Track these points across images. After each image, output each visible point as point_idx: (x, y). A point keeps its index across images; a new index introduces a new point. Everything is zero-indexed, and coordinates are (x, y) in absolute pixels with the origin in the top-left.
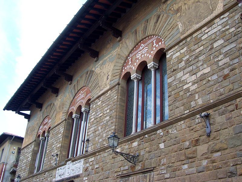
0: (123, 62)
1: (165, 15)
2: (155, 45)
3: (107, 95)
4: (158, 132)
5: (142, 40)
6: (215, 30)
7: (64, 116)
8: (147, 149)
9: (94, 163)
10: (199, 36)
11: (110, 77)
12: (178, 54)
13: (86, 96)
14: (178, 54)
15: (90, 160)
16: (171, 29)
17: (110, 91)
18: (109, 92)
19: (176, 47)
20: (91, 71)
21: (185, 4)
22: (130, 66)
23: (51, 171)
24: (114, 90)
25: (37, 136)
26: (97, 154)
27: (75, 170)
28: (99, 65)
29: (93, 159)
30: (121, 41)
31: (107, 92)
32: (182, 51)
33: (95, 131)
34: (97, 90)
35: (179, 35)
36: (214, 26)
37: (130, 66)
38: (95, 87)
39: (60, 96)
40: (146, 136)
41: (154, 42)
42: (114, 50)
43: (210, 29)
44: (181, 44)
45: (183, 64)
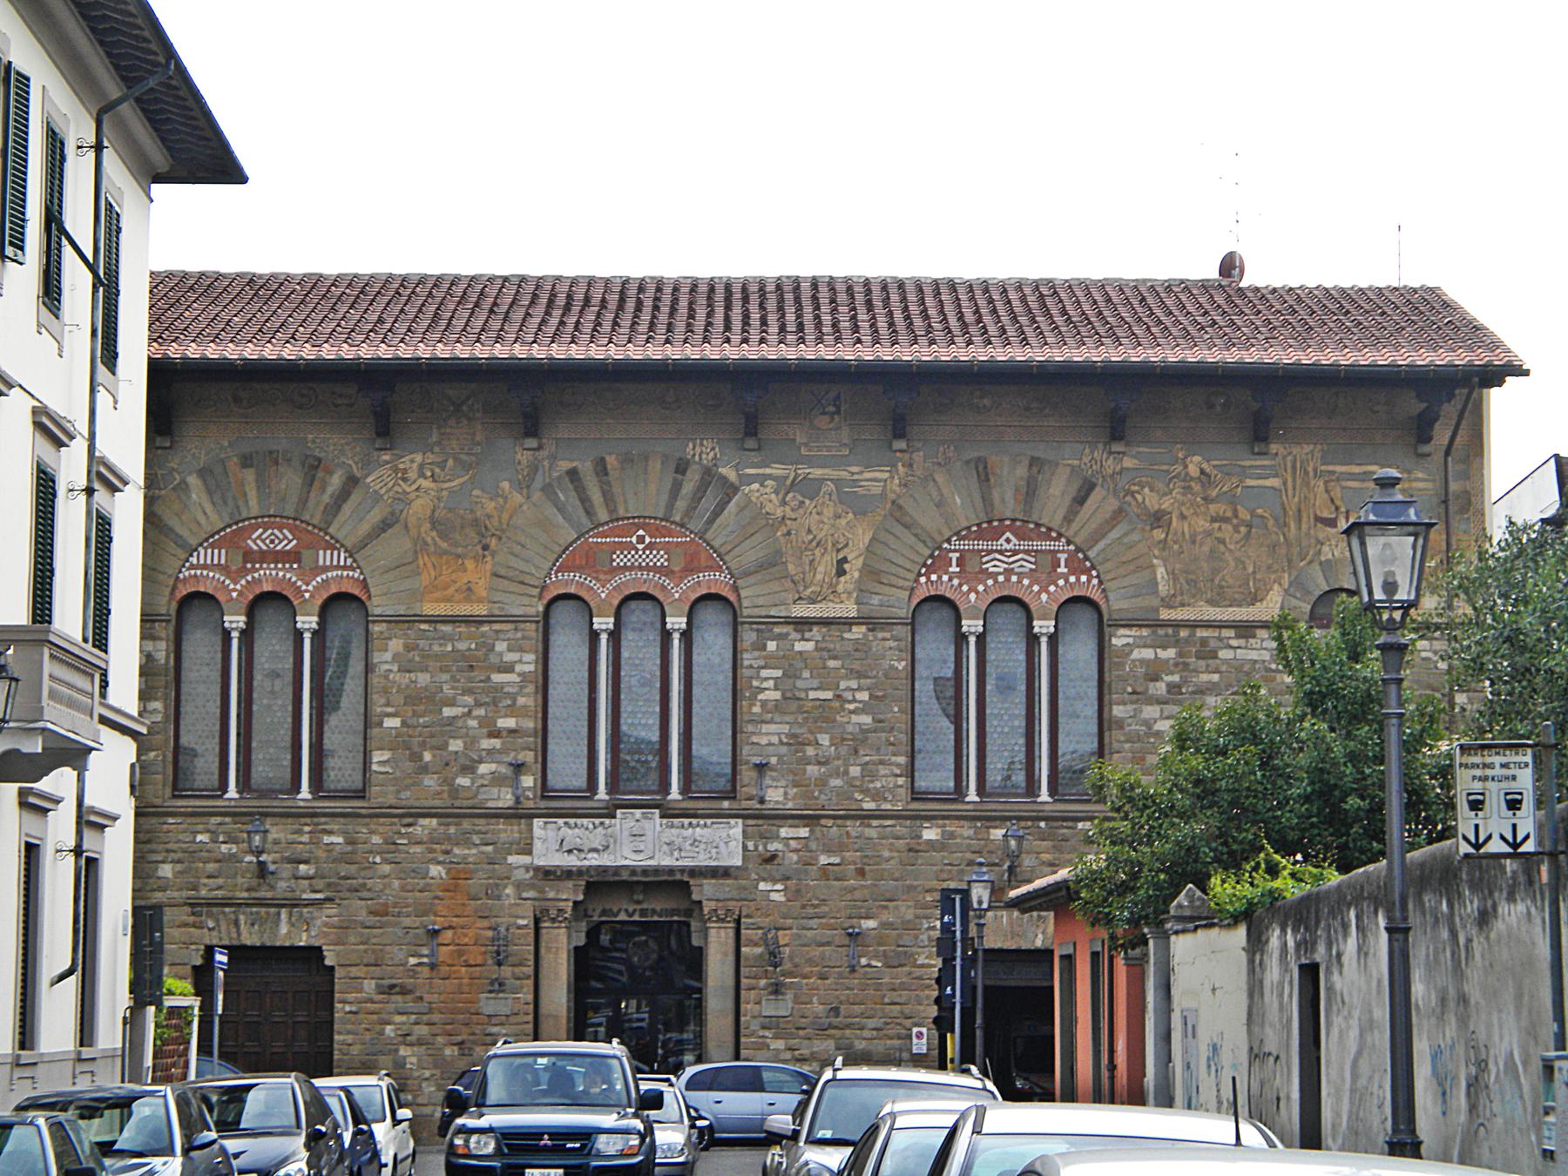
0: (927, 552)
1: (1113, 504)
2: (1062, 570)
3: (846, 635)
4: (1080, 825)
5: (1013, 520)
6: (1253, 655)
7: (526, 600)
8: (1046, 857)
9: (813, 846)
10: (1213, 644)
11: (853, 570)
12: (1148, 654)
13: (689, 570)
14: (1148, 654)
15: (784, 832)
16: (1132, 567)
17: (863, 629)
18: (854, 629)
19: (1145, 632)
20: (709, 474)
21: (1183, 517)
22: (956, 582)
23: (482, 821)
24: (888, 635)
26: (823, 822)
27: (687, 846)
28: (770, 477)
29: (804, 832)
30: (907, 456)
31: (848, 623)
32: (1162, 654)
33: (796, 742)
34: (775, 586)
35: (1156, 602)
36: (1251, 641)
37: (956, 582)
38: (762, 567)
39: (419, 458)
40: (1042, 824)
41: (1063, 557)
42: (868, 466)
43: (1242, 642)
44: (1161, 632)
45: (1160, 688)
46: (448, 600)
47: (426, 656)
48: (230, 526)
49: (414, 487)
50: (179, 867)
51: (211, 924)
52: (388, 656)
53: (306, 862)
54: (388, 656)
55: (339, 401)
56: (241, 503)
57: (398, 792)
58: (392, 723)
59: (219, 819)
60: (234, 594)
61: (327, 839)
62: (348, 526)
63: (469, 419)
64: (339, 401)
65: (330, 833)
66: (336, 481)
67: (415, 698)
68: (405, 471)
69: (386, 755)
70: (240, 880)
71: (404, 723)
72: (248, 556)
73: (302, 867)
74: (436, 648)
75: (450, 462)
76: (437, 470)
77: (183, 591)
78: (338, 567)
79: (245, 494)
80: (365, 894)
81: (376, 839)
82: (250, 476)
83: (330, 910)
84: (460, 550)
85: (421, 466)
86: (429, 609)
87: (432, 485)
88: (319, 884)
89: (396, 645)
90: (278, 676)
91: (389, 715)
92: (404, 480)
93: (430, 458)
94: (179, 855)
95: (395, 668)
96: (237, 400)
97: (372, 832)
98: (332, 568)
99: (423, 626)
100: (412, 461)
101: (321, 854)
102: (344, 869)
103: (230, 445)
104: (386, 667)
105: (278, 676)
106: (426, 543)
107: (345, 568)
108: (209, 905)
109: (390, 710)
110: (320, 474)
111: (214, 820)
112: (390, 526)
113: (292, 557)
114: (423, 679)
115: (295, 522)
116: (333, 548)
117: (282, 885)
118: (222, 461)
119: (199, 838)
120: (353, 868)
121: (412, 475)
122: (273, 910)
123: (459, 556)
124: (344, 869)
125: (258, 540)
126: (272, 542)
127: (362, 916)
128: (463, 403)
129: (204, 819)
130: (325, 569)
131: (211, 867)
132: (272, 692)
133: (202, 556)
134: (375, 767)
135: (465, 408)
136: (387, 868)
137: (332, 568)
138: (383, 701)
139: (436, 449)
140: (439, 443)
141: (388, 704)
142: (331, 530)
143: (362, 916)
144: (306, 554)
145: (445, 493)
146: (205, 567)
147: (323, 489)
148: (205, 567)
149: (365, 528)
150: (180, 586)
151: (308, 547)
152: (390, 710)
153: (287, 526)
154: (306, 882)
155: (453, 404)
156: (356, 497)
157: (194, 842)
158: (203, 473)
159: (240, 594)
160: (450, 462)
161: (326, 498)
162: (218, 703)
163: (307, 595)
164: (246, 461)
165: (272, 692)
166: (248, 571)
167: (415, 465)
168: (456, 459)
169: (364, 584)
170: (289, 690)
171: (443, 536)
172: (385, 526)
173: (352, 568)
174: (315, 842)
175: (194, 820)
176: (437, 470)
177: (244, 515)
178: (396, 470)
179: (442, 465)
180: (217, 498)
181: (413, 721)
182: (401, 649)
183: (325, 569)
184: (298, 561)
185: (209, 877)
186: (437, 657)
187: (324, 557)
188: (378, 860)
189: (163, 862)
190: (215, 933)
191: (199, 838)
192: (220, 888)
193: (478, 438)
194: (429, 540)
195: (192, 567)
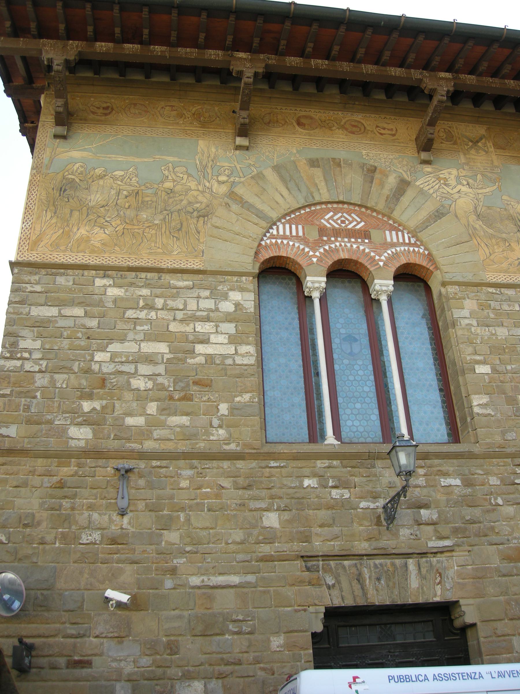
25: (257, 253)
46: (506, 271)
47: (498, 313)
48: (304, 207)
49: (455, 190)
50: (286, 516)
51: (330, 581)
52: (466, 313)
53: (426, 506)
54: (466, 313)
55: (382, 131)
56: (313, 189)
57: (503, 433)
58: (483, 369)
59: (327, 463)
60: (315, 260)
61: (444, 482)
62: (409, 211)
63: (487, 152)
64: (382, 131)
65: (446, 474)
66: (392, 181)
67: (498, 349)
68: (445, 179)
69: (485, 399)
70: (358, 528)
71: (494, 370)
72: (322, 231)
73: (423, 511)
74: (505, 307)
75: (479, 177)
76: (470, 181)
77: (266, 255)
78: (404, 244)
79: (316, 185)
80: (494, 538)
81: (494, 481)
82: (318, 173)
83: (460, 556)
84: (504, 235)
85: (458, 178)
86: (491, 277)
87: (470, 190)
88: (444, 530)
89: (470, 305)
90: (356, 340)
91: (479, 362)
92: (445, 185)
93: (464, 173)
94: (286, 501)
95: (475, 323)
96: (299, 124)
97: (487, 473)
98: (398, 244)
99: (491, 290)
100: (450, 174)
101: (441, 497)
102: (468, 513)
103: (298, 152)
104: (467, 321)
105: (356, 340)
106: (475, 229)
107: (410, 244)
108: (326, 557)
109: (478, 358)
110: (377, 175)
111: (319, 464)
112: (443, 215)
113: (365, 234)
114: (502, 332)
115: (362, 207)
116: (397, 230)
117: (405, 533)
118: (294, 162)
119: (307, 482)
120: (477, 512)
121: (452, 182)
122: (398, 562)
123: (505, 240)
124: (468, 513)
125: (330, 220)
126: (343, 222)
127: (496, 562)
128: (478, 142)
129: (310, 463)
130: (393, 245)
131: (323, 514)
132: (351, 354)
133: (281, 229)
134: (476, 410)
135: (480, 144)
136: (510, 510)
137: (398, 244)
138: (470, 350)
139: (466, 167)
140: (467, 164)
141: (476, 353)
142: (396, 214)
143: (496, 562)
144: (374, 233)
145: (480, 196)
146: (284, 237)
147: (382, 185)
148: (284, 237)
149: (423, 215)
150: (263, 251)
151: (376, 227)
152: (478, 358)
153: (354, 211)
154: (430, 528)
155: (472, 141)
156: (410, 194)
157: (301, 486)
158: (277, 168)
159: (320, 260)
160: (479, 177)
161: (386, 191)
162: (300, 362)
163: (381, 264)
164: (313, 163)
165: (351, 354)
166: (326, 242)
167: (452, 177)
168: (483, 175)
169: (430, 257)
170: (367, 352)
171: (490, 226)
172: (438, 215)
173: (415, 245)
174: (431, 485)
175: (299, 463)
176: (470, 181)
177: (317, 199)
178: (439, 179)
179: (474, 177)
180: (291, 185)
181: (501, 368)
182: (475, 307)
183: (393, 245)
184: (369, 238)
185: (320, 526)
186: (508, 315)
187: (390, 236)
188: (500, 501)
189: (267, 510)
190: (335, 592)
191: (307, 482)
192: (336, 538)
193: (496, 163)
194: (477, 226)
195: (273, 237)
